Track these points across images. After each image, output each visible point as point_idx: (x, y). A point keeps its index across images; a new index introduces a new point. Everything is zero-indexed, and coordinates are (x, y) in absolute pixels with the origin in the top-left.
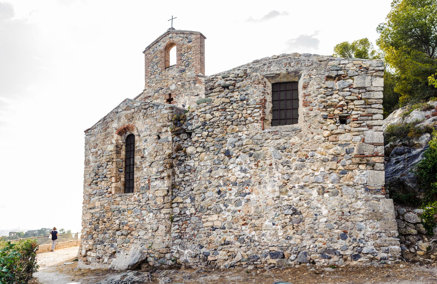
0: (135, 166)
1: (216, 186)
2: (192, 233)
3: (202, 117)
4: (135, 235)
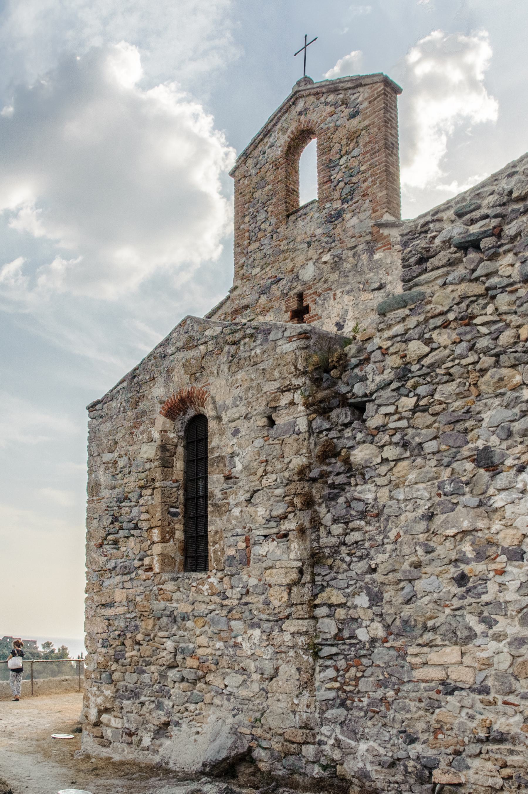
0: (209, 502)
1: (451, 562)
2: (379, 694)
3: (395, 353)
4: (216, 683)
